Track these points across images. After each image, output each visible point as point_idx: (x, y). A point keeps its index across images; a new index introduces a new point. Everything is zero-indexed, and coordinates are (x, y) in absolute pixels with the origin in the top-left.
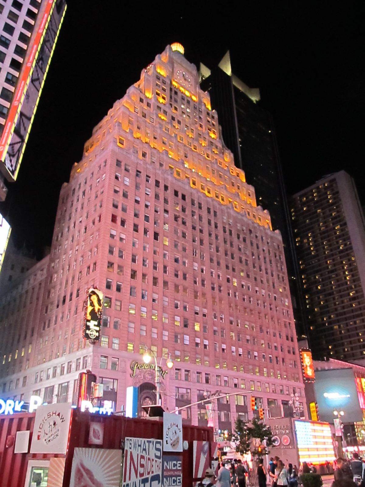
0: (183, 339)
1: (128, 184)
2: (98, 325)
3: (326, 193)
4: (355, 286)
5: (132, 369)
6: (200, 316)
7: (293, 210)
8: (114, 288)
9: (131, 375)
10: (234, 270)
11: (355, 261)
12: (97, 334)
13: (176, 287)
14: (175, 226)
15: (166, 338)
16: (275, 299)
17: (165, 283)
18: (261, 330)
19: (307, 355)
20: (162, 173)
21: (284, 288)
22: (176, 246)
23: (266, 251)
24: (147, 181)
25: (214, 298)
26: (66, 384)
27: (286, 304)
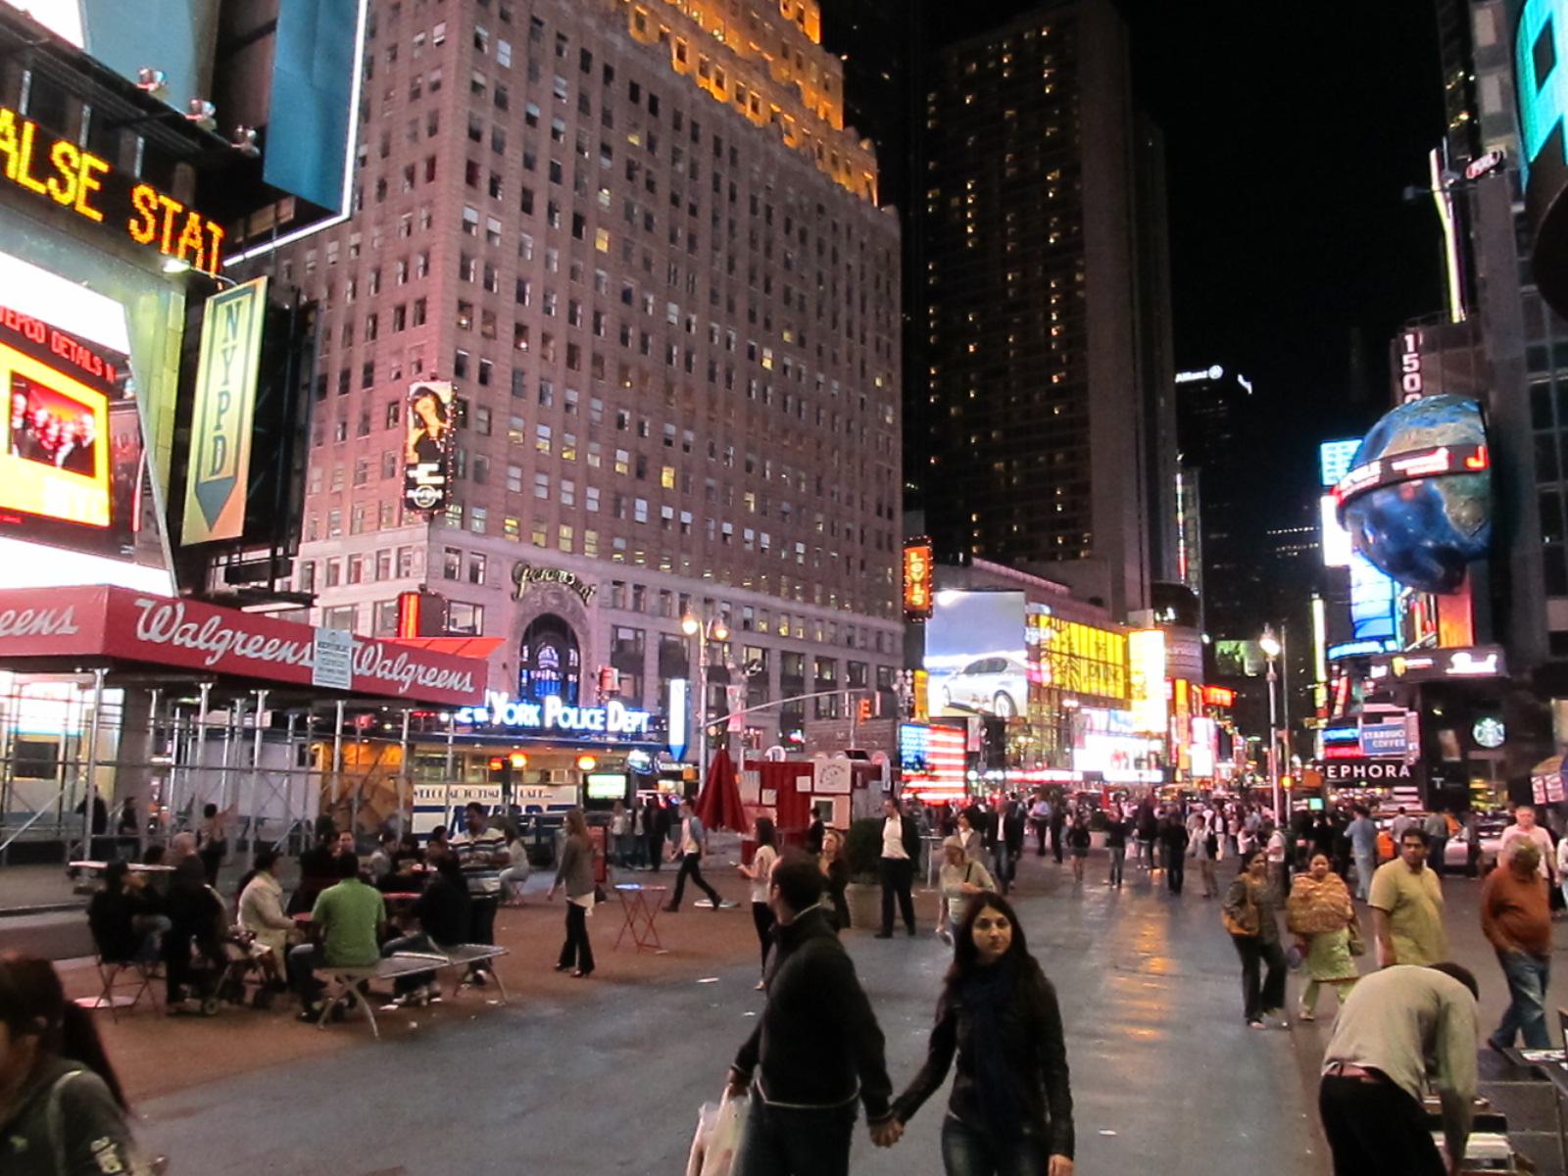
0: (632, 509)
1: (506, 62)
2: (442, 472)
3: (1041, 60)
4: (1070, 358)
5: (517, 580)
6: (676, 449)
7: (931, 98)
8: (474, 373)
9: (514, 597)
10: (768, 324)
11: (1081, 286)
12: (439, 494)
13: (623, 371)
14: (628, 194)
15: (593, 506)
16: (862, 408)
17: (597, 360)
18: (819, 489)
19: (919, 556)
20: (599, 27)
21: (889, 376)
22: (627, 253)
23: (856, 270)
24: (559, 52)
25: (712, 404)
26: (349, 609)
27: (889, 420)
